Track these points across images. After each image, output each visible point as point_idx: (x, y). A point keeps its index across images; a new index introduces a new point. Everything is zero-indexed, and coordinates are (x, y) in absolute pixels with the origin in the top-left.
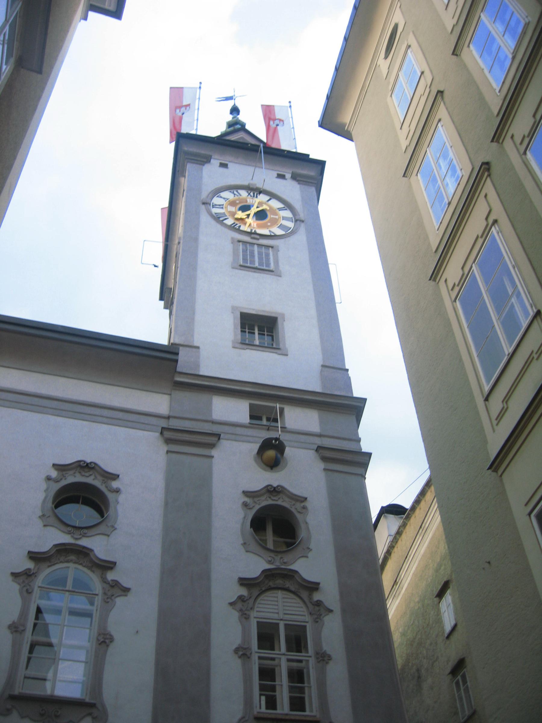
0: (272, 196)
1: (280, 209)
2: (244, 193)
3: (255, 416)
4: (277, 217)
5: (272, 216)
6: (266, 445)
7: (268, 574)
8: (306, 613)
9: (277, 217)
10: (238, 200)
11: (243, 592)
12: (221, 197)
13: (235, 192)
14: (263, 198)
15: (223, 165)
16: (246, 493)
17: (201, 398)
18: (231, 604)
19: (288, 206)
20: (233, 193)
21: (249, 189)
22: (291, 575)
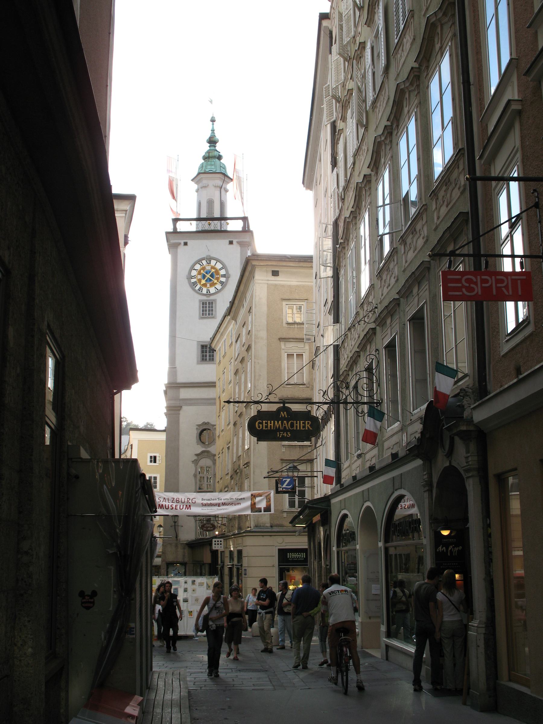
0: (218, 260)
1: (220, 269)
4: (218, 276)
5: (217, 276)
7: (203, 452)
8: (212, 464)
9: (218, 276)
10: (202, 269)
11: (196, 458)
12: (195, 270)
13: (201, 264)
16: (198, 425)
18: (193, 461)
20: (200, 264)
22: (208, 452)
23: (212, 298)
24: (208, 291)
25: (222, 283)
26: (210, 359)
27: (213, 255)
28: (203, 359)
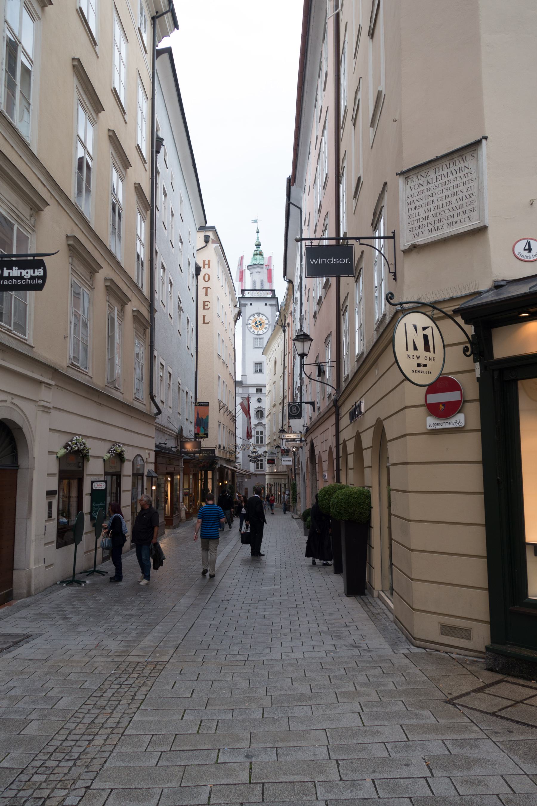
0: (263, 315)
2: (256, 315)
3: (257, 390)
6: (259, 399)
7: (258, 423)
14: (261, 316)
15: (251, 304)
17: (247, 388)
19: (267, 319)
21: (257, 314)
23: (260, 336)
24: (258, 332)
25: (266, 328)
26: (259, 371)
27: (261, 312)
28: (256, 371)
